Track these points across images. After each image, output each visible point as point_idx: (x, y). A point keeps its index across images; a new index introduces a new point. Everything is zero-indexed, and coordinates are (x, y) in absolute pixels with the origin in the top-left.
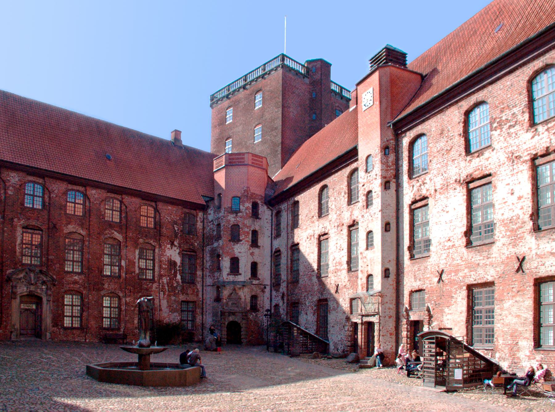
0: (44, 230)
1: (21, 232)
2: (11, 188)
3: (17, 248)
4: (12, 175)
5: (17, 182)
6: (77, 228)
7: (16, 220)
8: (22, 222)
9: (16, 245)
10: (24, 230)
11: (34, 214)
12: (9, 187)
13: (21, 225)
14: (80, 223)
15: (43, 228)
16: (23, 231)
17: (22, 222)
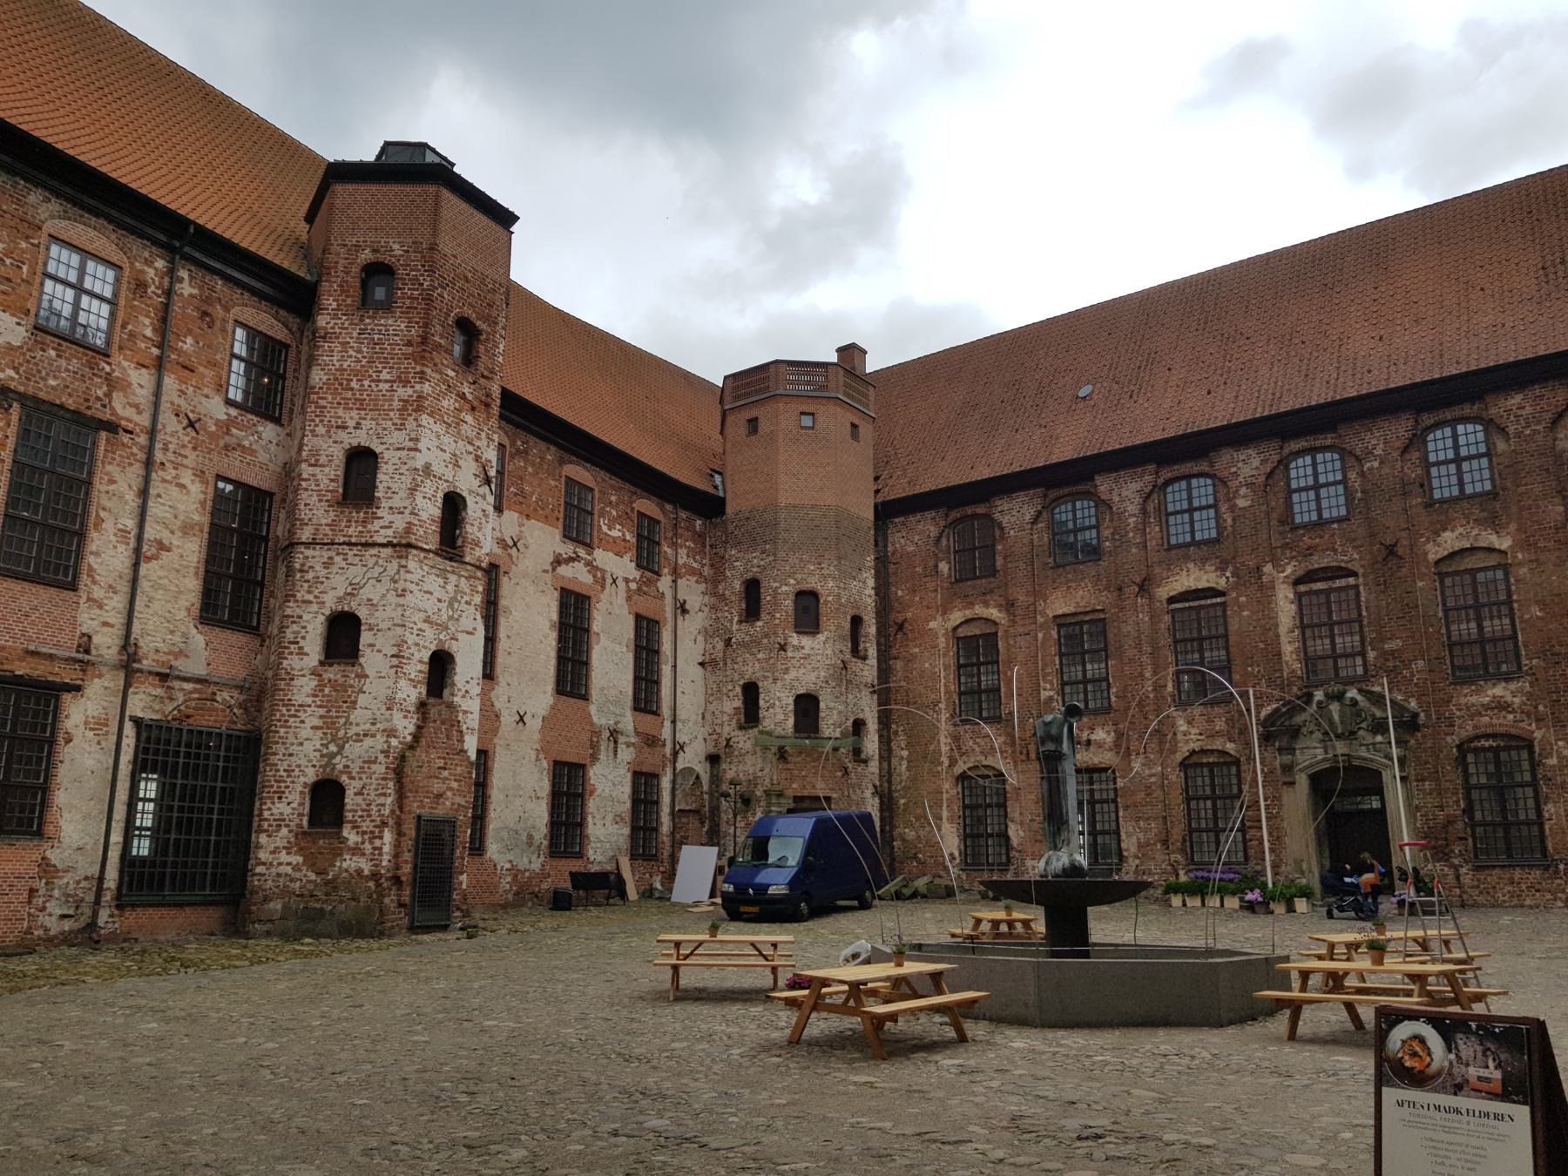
0: (1361, 571)
1: (1291, 596)
2: (1243, 491)
3: (1284, 639)
4: (1242, 457)
5: (1257, 468)
6: (1475, 532)
7: (1268, 568)
8: (1289, 570)
9: (1278, 636)
10: (1302, 588)
11: (1322, 537)
12: (1237, 491)
13: (1286, 577)
14: (1485, 514)
15: (1356, 567)
16: (1296, 593)
17: (1289, 570)
